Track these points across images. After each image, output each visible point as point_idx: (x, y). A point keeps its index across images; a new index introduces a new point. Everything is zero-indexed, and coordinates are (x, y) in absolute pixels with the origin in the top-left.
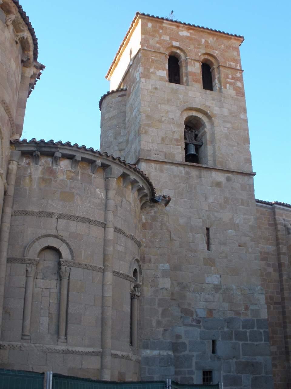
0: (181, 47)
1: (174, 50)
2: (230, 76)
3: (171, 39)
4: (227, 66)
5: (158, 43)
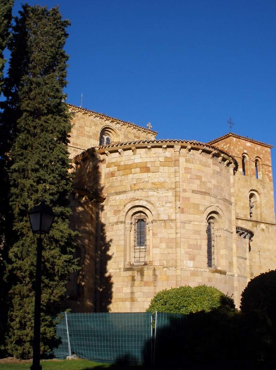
0: (247, 153)
1: (244, 155)
2: (267, 170)
3: (243, 148)
4: (266, 164)
5: (239, 151)
